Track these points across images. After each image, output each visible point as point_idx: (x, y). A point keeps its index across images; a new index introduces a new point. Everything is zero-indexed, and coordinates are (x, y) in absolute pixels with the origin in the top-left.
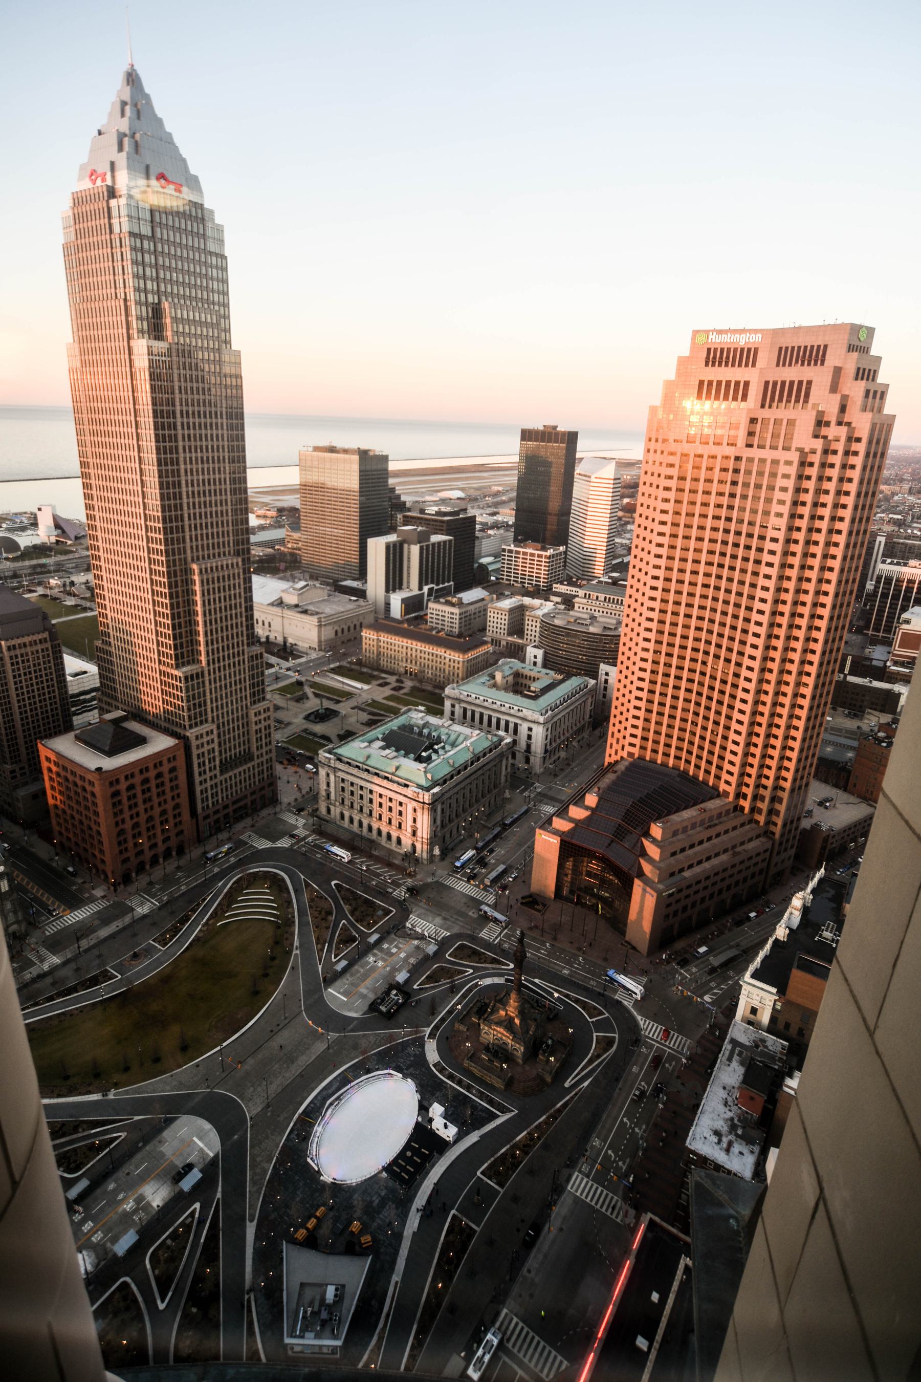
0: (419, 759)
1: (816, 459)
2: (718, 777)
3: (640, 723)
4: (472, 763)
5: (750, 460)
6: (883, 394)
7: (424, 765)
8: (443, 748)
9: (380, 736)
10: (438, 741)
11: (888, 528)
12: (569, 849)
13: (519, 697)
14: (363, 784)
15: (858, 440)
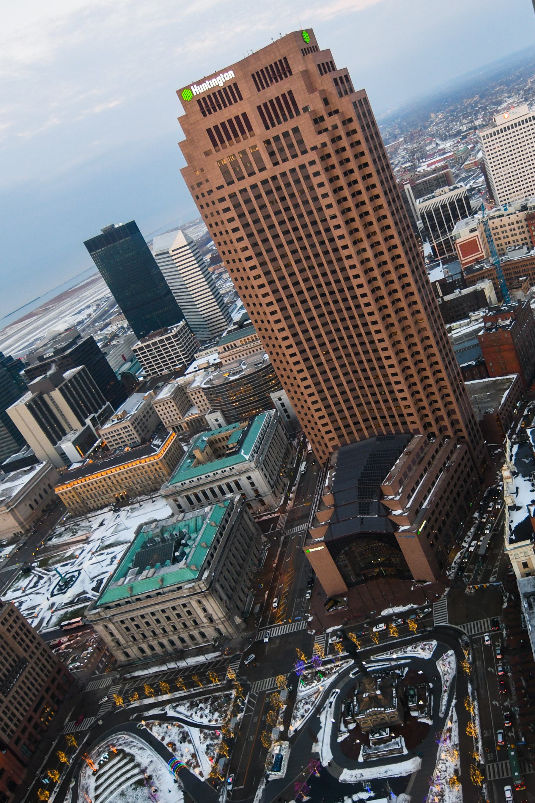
0: (175, 560)
1: (330, 149)
2: (404, 423)
3: (327, 420)
4: (221, 534)
5: (283, 174)
6: (347, 77)
7: (184, 561)
8: (190, 538)
9: (130, 565)
10: (182, 536)
11: (407, 176)
12: (334, 546)
13: (224, 459)
14: (142, 612)
15: (350, 120)
